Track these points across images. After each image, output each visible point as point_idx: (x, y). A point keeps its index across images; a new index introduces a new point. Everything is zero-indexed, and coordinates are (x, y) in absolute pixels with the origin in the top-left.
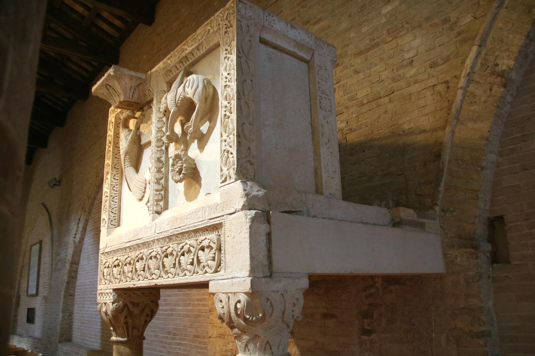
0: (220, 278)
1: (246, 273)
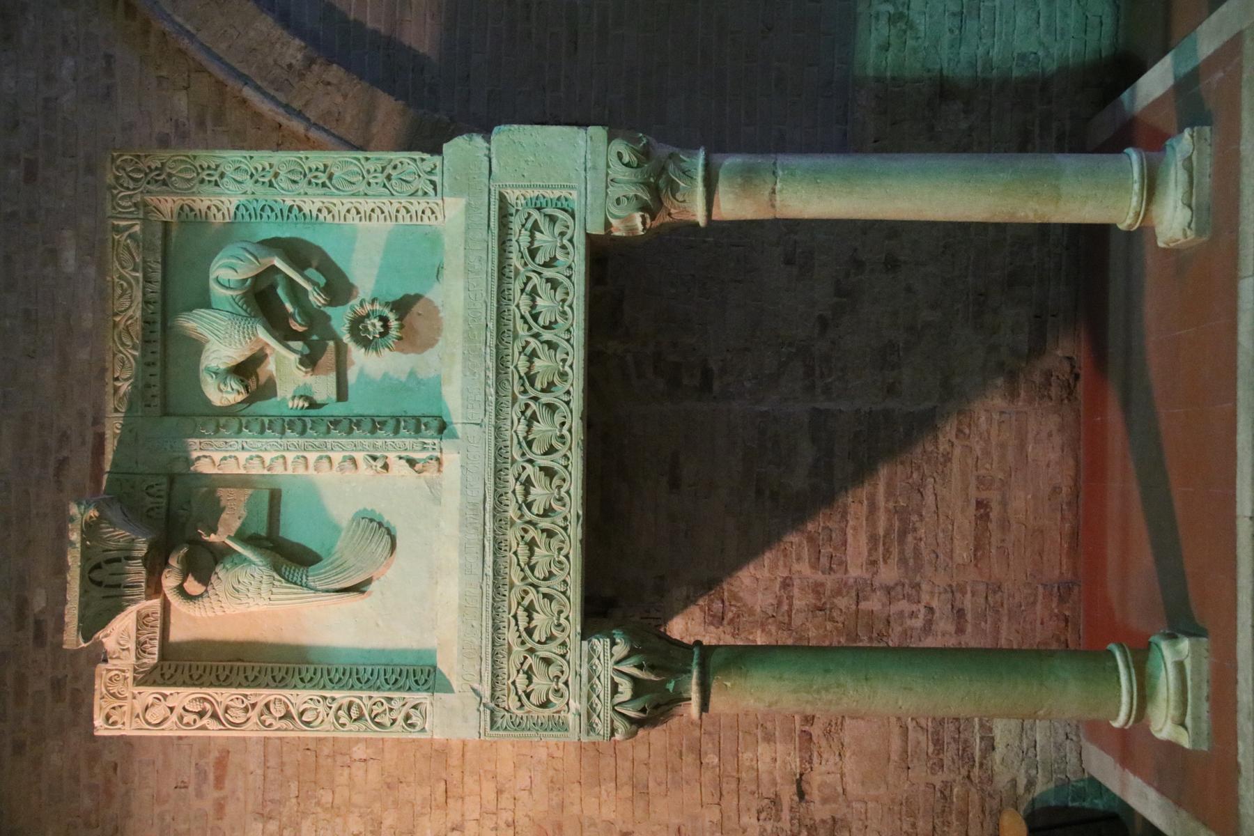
0: (583, 208)
1: (580, 135)
